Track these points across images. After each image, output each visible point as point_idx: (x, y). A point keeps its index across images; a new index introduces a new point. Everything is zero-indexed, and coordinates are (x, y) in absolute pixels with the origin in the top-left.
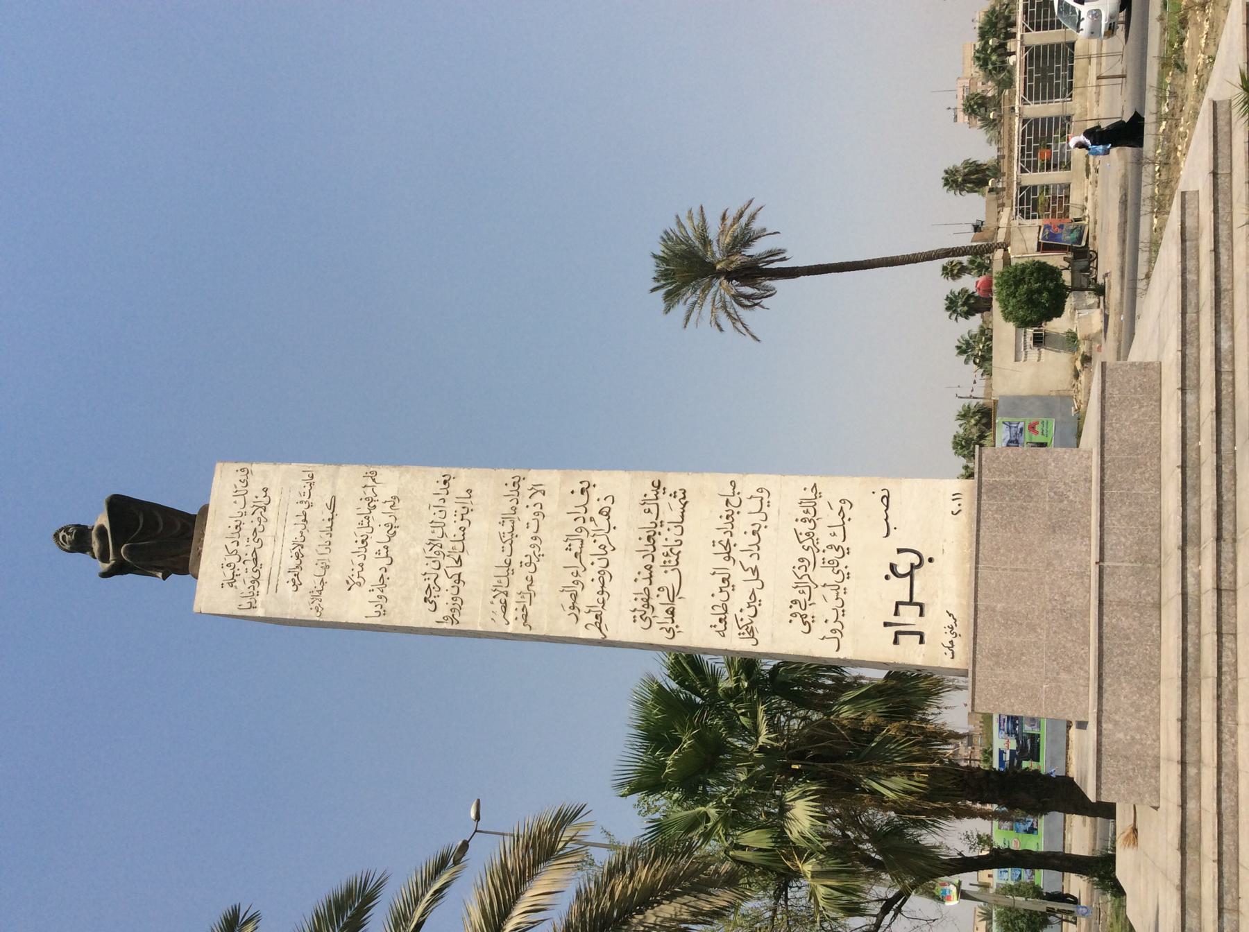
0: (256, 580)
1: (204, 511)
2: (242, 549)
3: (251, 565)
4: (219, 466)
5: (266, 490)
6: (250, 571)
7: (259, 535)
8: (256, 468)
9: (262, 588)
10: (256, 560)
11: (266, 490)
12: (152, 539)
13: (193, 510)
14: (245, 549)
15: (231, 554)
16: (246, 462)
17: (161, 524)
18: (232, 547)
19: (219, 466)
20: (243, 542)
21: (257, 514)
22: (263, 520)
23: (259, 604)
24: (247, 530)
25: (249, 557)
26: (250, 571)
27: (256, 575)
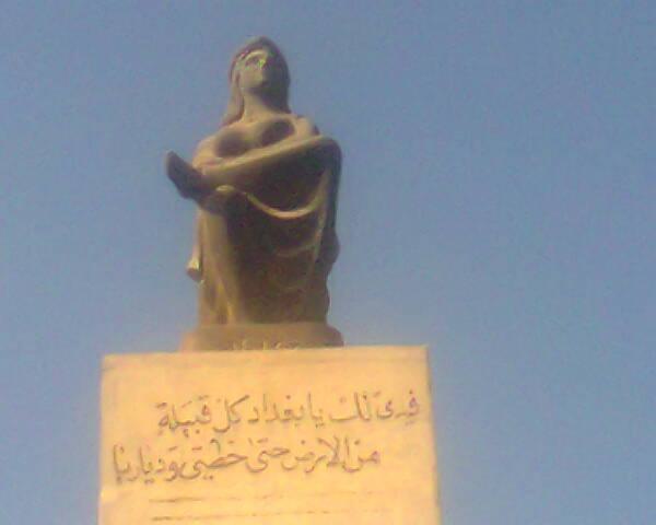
0: (177, 472)
1: (333, 339)
2: (246, 432)
3: (210, 456)
4: (418, 352)
5: (374, 458)
6: (198, 456)
7: (274, 463)
8: (422, 431)
9: (161, 489)
10: (219, 464)
11: (374, 458)
12: (273, 248)
13: (334, 318)
14: (245, 440)
15: (230, 409)
16: (434, 407)
17: (302, 212)
18: (246, 411)
19: (418, 352)
20: (255, 432)
21: (320, 451)
22: (309, 463)
23: (127, 487)
24: (281, 436)
25: (227, 449)
26: (198, 456)
27: (188, 471)
